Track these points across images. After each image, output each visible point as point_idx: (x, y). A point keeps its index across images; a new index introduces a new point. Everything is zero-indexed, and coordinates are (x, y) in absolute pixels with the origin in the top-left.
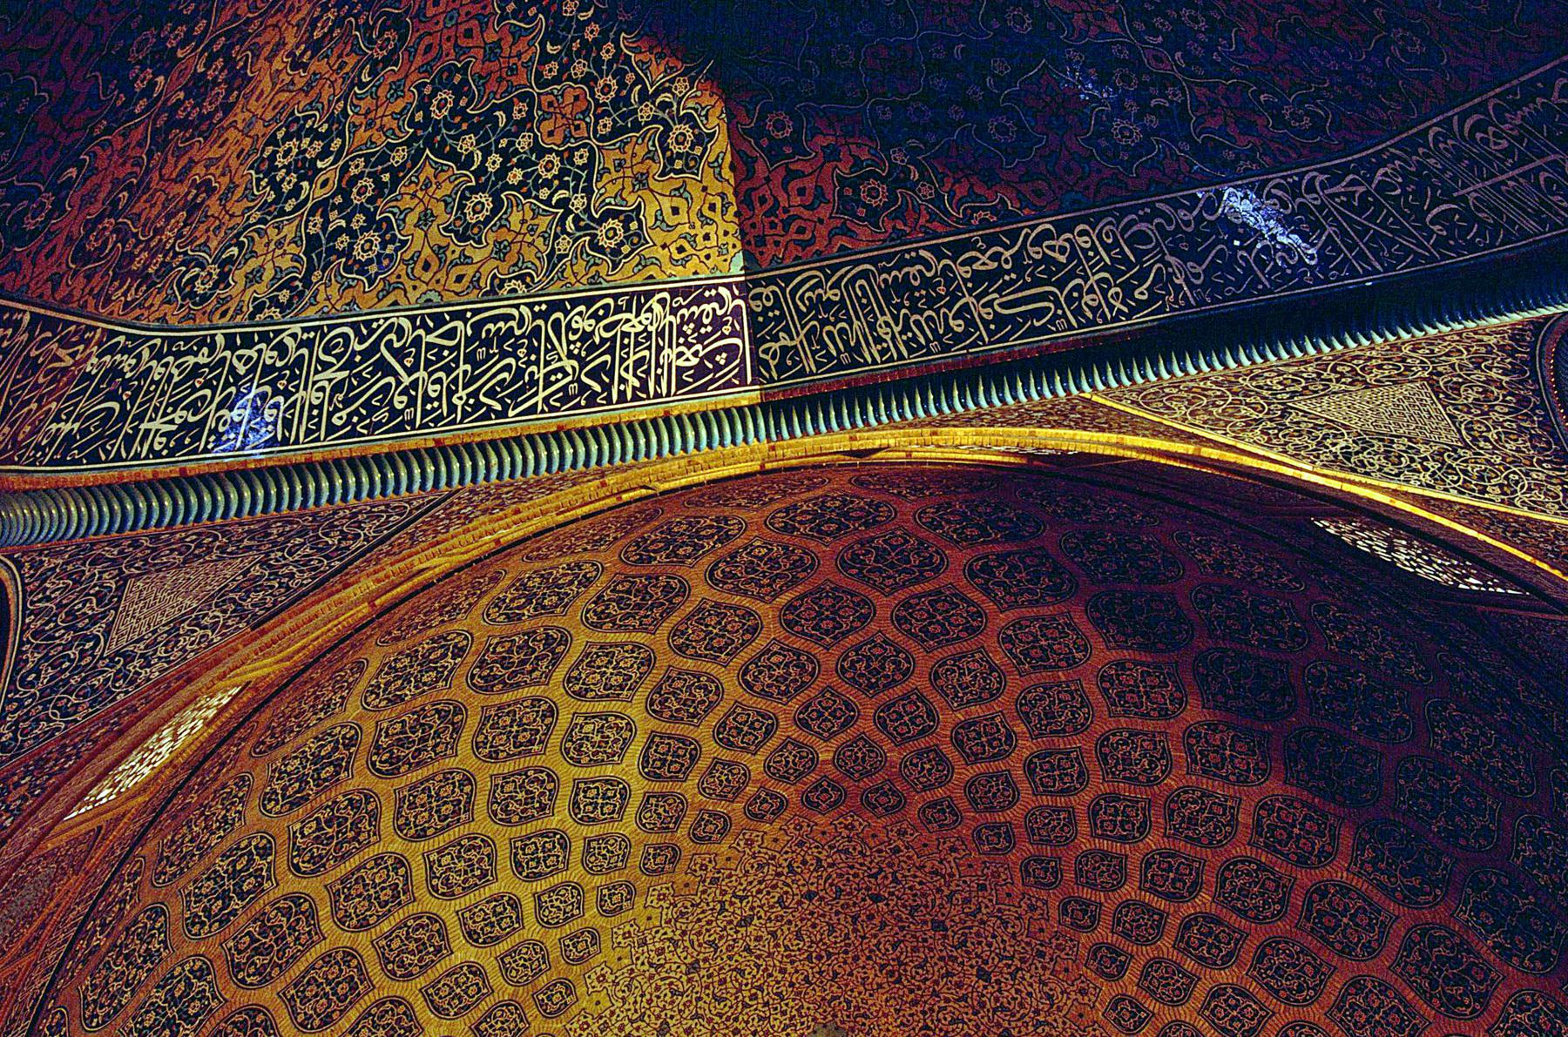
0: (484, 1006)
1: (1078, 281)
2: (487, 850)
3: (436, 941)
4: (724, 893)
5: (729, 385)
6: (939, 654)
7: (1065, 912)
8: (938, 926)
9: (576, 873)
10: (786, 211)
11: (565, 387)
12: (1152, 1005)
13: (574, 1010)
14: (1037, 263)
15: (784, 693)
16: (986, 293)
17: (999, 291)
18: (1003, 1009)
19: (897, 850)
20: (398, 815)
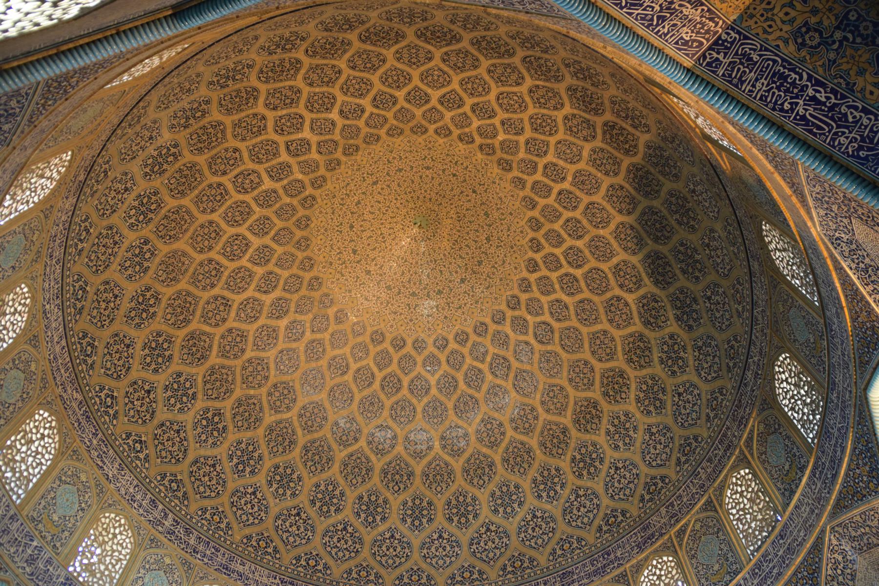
0: (327, 137)
1: (847, 131)
2: (369, 87)
3: (329, 106)
5: (687, 55)
6: (568, 138)
8: (487, 214)
10: (773, 15)
11: (647, 15)
12: (535, 288)
13: (353, 158)
14: (840, 113)
15: (507, 110)
16: (809, 105)
17: (815, 109)
18: (486, 254)
19: (494, 183)
20: (353, 56)
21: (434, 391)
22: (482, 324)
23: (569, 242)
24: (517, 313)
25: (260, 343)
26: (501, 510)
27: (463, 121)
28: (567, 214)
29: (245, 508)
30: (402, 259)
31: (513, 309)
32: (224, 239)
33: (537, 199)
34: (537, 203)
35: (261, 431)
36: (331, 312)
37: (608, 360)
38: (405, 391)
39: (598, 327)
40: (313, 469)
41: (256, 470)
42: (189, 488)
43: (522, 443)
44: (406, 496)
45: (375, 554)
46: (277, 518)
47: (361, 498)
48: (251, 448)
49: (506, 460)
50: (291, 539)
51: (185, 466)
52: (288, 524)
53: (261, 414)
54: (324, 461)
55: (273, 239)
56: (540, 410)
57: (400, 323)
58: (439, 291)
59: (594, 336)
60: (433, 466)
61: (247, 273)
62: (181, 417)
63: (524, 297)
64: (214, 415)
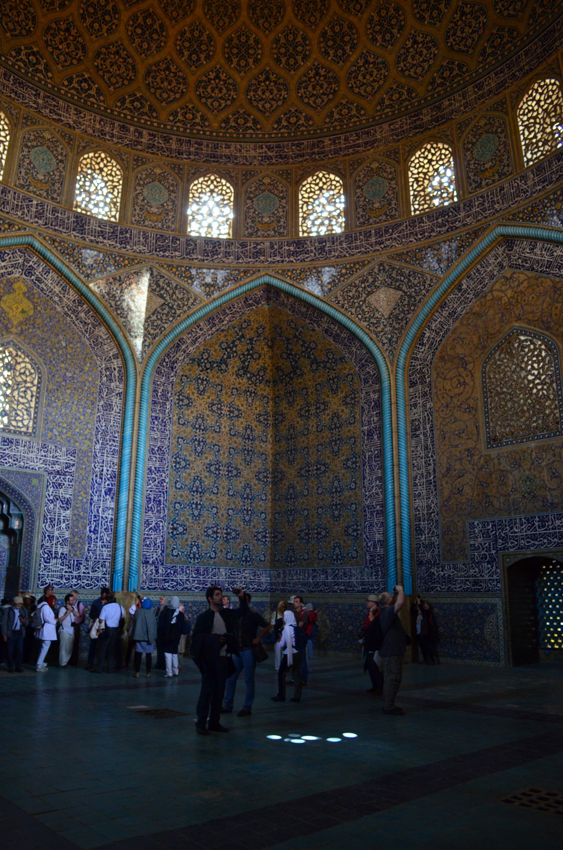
29: (213, 95)
41: (211, 53)
45: (352, 87)
46: (248, 91)
50: (267, 106)
52: (260, 92)
62: (113, 38)
64: (145, 18)
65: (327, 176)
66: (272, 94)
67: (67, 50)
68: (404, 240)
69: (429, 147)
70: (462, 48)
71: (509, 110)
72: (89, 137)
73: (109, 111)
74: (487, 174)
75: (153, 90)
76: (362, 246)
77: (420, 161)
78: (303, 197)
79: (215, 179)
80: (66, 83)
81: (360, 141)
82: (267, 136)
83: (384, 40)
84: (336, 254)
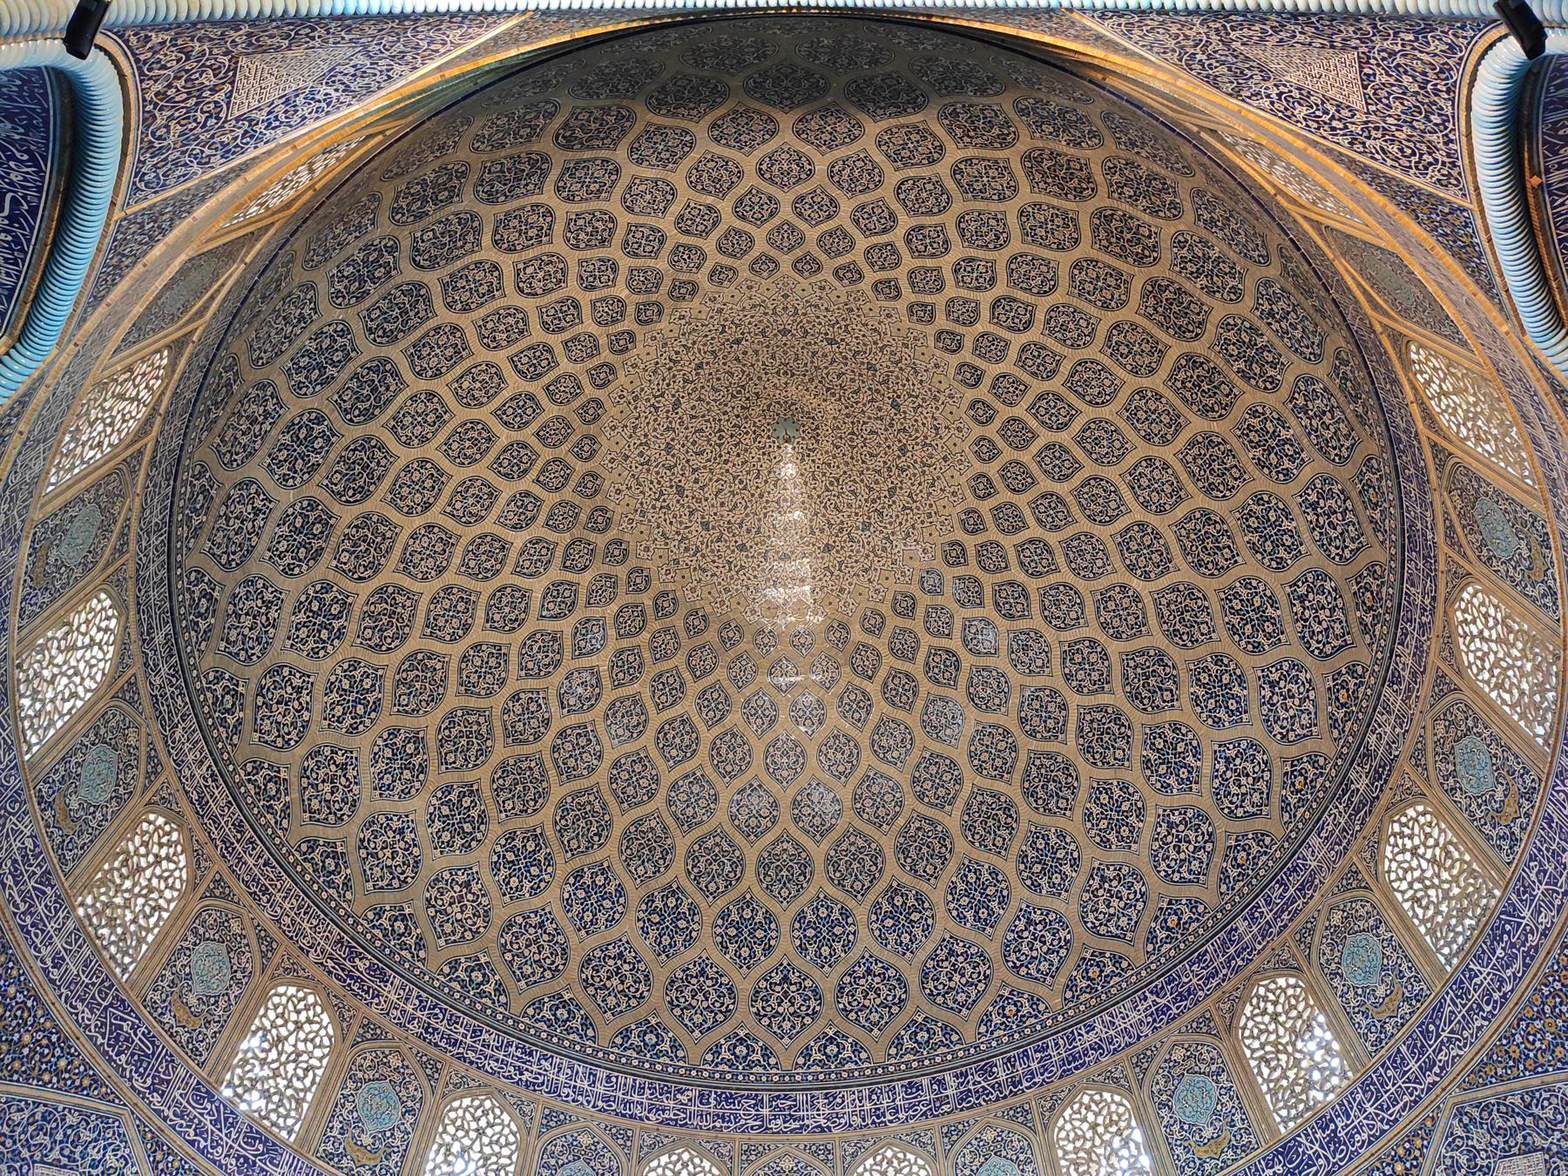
4: (648, 400)
7: (841, 279)
8: (785, 332)
9: (547, 454)
13: (616, 517)
19: (720, 311)
21: (1053, 539)
22: (972, 406)
23: (843, 219)
24: (968, 343)
25: (841, 769)
26: (1282, 553)
27: (584, 347)
28: (786, 212)
30: (832, 484)
31: (960, 347)
32: (654, 753)
33: (755, 253)
34: (763, 254)
35: (961, 845)
36: (857, 635)
37: (1077, 229)
38: (1033, 585)
39: (1013, 221)
40: (1062, 804)
42: (945, 1016)
43: (1192, 443)
44: (1187, 689)
47: (1147, 762)
48: (972, 877)
49: (1209, 489)
50: (1123, 922)
51: (916, 997)
52: (1102, 908)
53: (939, 828)
54: (1063, 778)
55: (697, 678)
56: (1145, 382)
57: (926, 535)
58: (900, 449)
59: (1029, 234)
60: (1167, 614)
61: (727, 738)
62: (855, 954)
63: (941, 322)
65: (1272, 986)
66: (1121, 899)
67: (792, 1010)
68: (1466, 1034)
69: (1396, 827)
70: (1335, 643)
71: (1456, 679)
72: (859, 1133)
73: (880, 1071)
74: (1510, 810)
75: (940, 1000)
76: (1401, 1092)
77: (1400, 863)
78: (1253, 1051)
79: (1092, 1100)
80: (801, 1061)
81: (1292, 890)
82: (1144, 973)
83: (1231, 713)
84: (1365, 1136)
